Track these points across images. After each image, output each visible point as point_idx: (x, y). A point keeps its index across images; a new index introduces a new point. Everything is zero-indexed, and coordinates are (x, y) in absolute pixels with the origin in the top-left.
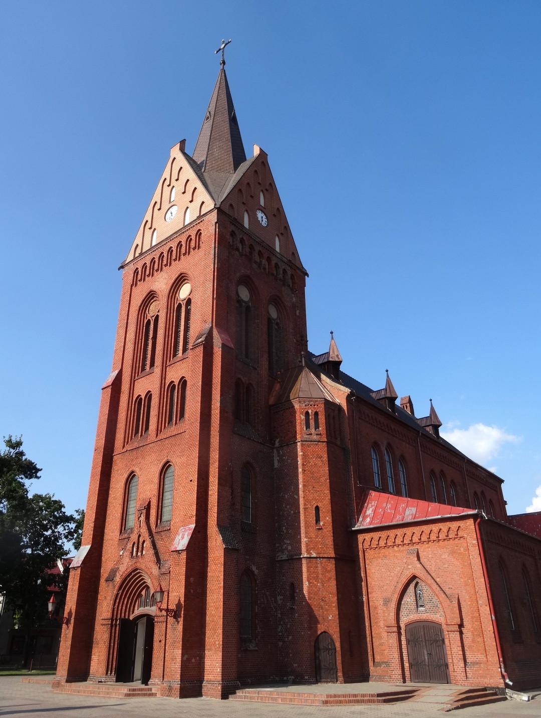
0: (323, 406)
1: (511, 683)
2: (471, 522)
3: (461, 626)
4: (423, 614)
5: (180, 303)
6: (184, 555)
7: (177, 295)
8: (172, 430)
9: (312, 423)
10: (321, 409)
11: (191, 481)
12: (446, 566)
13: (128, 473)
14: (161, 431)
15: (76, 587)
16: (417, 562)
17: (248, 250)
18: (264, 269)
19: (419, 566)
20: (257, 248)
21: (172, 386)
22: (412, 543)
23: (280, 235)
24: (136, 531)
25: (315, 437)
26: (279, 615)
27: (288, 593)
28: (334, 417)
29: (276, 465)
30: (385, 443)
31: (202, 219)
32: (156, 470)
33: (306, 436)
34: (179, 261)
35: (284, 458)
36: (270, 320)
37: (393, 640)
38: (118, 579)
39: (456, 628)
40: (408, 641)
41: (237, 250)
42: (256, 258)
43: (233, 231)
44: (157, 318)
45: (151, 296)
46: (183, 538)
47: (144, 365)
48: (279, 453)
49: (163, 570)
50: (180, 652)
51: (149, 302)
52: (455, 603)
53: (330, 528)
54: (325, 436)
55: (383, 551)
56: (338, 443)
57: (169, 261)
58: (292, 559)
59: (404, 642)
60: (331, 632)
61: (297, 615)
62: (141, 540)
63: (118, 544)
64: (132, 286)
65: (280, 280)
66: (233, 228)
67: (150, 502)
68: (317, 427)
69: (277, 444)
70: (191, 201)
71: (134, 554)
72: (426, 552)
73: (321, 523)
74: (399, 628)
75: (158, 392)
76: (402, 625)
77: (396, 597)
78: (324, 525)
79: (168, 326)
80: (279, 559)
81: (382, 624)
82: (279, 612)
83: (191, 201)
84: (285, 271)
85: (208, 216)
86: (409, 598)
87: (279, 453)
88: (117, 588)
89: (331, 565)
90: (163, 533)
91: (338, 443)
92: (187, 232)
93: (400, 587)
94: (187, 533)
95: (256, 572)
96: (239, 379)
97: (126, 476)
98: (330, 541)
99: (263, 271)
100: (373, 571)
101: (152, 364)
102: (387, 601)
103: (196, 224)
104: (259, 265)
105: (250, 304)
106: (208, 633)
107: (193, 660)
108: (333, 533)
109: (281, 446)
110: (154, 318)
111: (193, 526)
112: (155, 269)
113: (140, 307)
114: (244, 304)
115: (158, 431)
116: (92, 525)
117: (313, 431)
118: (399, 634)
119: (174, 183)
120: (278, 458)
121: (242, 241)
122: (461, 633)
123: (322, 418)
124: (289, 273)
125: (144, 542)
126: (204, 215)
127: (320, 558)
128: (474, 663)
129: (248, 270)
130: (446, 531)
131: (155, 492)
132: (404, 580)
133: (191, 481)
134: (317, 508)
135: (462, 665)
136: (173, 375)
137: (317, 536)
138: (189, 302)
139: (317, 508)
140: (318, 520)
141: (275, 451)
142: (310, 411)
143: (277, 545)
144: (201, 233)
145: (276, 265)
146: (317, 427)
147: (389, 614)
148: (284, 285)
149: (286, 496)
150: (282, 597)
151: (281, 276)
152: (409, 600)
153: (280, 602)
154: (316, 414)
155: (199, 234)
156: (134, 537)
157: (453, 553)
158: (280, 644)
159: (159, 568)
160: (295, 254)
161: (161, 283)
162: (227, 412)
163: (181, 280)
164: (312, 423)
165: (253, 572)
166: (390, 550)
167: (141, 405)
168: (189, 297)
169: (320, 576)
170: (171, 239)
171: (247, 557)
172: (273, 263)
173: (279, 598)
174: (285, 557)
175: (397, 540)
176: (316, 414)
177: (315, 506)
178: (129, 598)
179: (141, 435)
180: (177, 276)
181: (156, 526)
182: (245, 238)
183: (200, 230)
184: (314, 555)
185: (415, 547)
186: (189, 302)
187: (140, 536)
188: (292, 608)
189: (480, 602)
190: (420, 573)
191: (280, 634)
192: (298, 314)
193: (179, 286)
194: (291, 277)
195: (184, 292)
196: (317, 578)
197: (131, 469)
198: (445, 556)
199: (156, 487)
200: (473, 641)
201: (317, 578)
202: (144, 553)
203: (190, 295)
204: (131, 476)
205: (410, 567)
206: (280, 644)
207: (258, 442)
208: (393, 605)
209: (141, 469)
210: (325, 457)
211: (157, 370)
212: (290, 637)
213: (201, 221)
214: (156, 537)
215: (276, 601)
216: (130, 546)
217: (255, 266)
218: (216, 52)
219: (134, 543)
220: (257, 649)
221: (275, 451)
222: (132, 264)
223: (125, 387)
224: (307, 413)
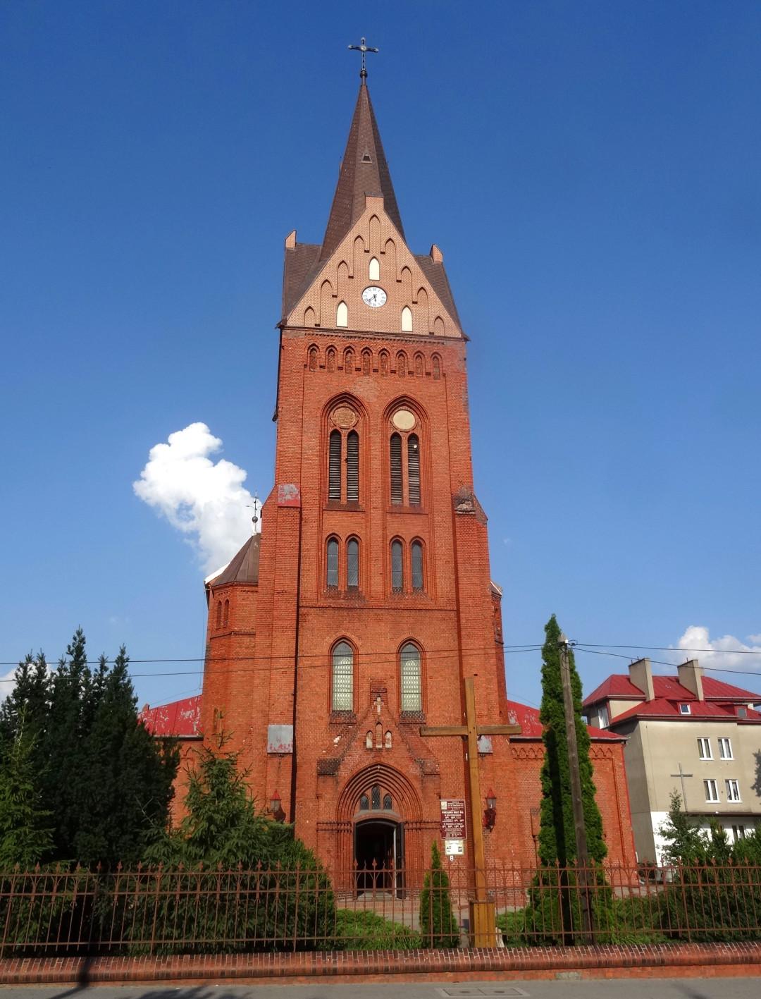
11: (476, 675)
13: (335, 637)
31: (442, 341)
64: (305, 366)
92: (415, 345)
103: (430, 342)
133: (476, 675)
138: (413, 438)
155: (435, 356)
168: (416, 432)
180: (398, 395)
193: (395, 409)
197: (340, 634)
209: (360, 638)
211: (376, 515)
218: (350, 46)
222: (304, 332)
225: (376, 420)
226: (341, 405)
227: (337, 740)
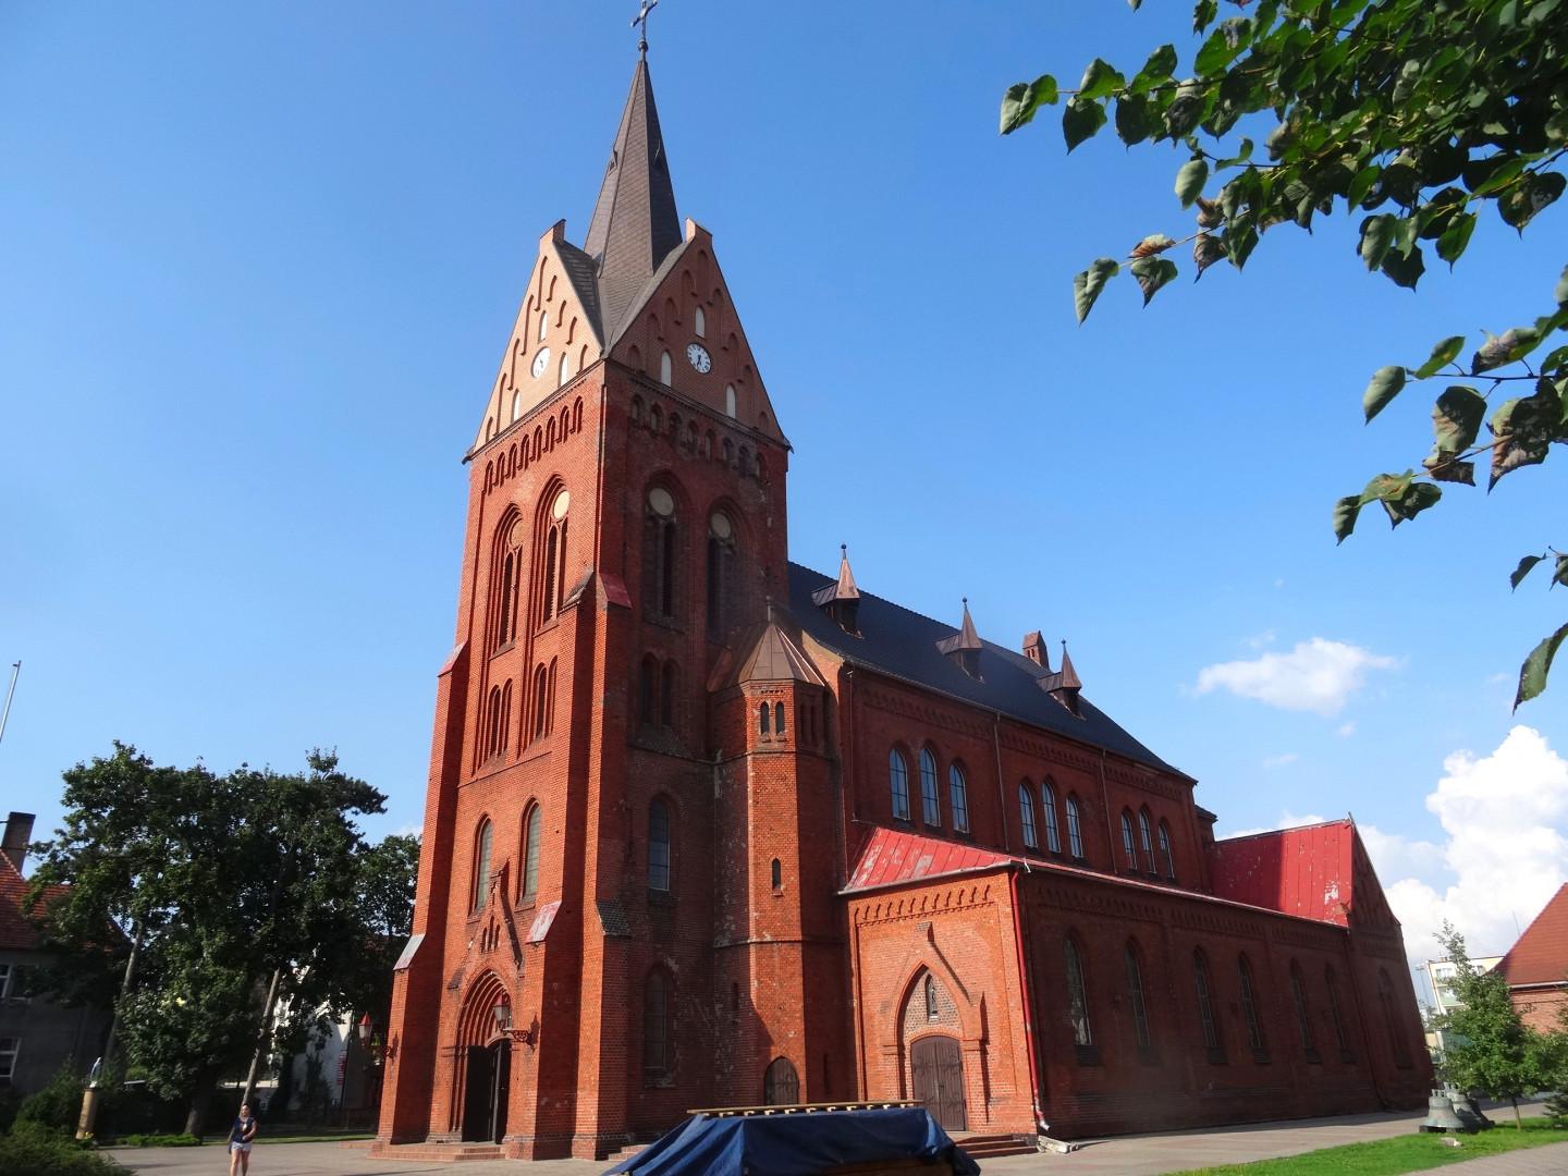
0: (791, 692)
1: (1046, 1127)
2: (1005, 876)
3: (984, 1041)
4: (936, 1026)
6: (542, 949)
7: (551, 512)
9: (772, 721)
10: (788, 697)
12: (970, 949)
14: (525, 747)
15: (403, 1001)
16: (928, 944)
17: (666, 424)
18: (702, 453)
19: (931, 949)
20: (686, 417)
23: (736, 384)
25: (776, 746)
26: (717, 1034)
27: (729, 999)
28: (813, 710)
29: (717, 793)
30: (921, 741)
32: (516, 811)
33: (762, 745)
35: (729, 781)
36: (713, 544)
37: (891, 1066)
38: (464, 986)
39: (977, 1045)
40: (914, 1069)
42: (685, 434)
43: (637, 396)
45: (511, 514)
46: (543, 922)
48: (721, 772)
50: (535, 1093)
51: (511, 522)
52: (977, 1005)
53: (796, 894)
54: (792, 742)
55: (884, 926)
56: (820, 751)
58: (736, 946)
59: (908, 1070)
60: (792, 1056)
61: (741, 1032)
63: (466, 931)
64: (483, 494)
66: (637, 389)
67: (508, 864)
68: (780, 728)
69: (719, 759)
70: (569, 343)
71: (486, 947)
73: (782, 887)
74: (901, 1047)
76: (907, 1043)
77: (897, 1000)
78: (786, 889)
79: (535, 567)
82: (717, 1028)
83: (569, 343)
86: (917, 1002)
87: (721, 772)
88: (462, 999)
89: (796, 954)
90: (525, 914)
91: (820, 751)
93: (904, 983)
94: (548, 916)
95: (675, 968)
97: (476, 821)
98: (795, 914)
99: (698, 457)
100: (869, 959)
102: (886, 1006)
105: (675, 519)
106: (582, 1065)
107: (558, 1105)
108: (801, 901)
111: (558, 903)
112: (530, 456)
113: (496, 531)
114: (661, 522)
115: (521, 748)
116: (427, 901)
117: (773, 735)
118: (901, 1056)
119: (545, 305)
120: (720, 782)
121: (656, 409)
122: (984, 1052)
123: (789, 714)
126: (588, 368)
127: (777, 942)
128: (1000, 1099)
131: (516, 848)
132: (909, 972)
134: (776, 863)
135: (982, 1102)
137: (774, 908)
139: (776, 863)
140: (776, 882)
141: (716, 768)
142: (769, 702)
143: (716, 924)
145: (727, 442)
146: (780, 728)
147: (887, 1027)
150: (721, 1006)
152: (916, 1003)
153: (718, 1013)
154: (780, 705)
155: (579, 403)
156: (486, 921)
157: (979, 928)
158: (718, 1077)
159: (519, 968)
161: (524, 490)
162: (617, 717)
163: (553, 487)
164: (772, 721)
165: (669, 969)
166: (894, 925)
167: (497, 700)
169: (777, 971)
171: (659, 946)
172: (720, 438)
173: (718, 1006)
174: (726, 943)
175: (902, 910)
176: (780, 705)
177: (772, 859)
178: (482, 1015)
179: (499, 754)
180: (547, 479)
181: (517, 902)
182: (661, 404)
184: (768, 938)
187: (493, 918)
188: (734, 1022)
189: (1011, 1004)
191: (718, 1062)
196: (771, 975)
197: (482, 811)
198: (969, 933)
199: (516, 840)
200: (1001, 1063)
201: (771, 975)
204: (484, 823)
205: (918, 952)
206: (718, 1077)
208: (893, 1012)
210: (792, 776)
211: (520, 644)
212: (732, 1067)
214: (517, 919)
215: (712, 1012)
216: (480, 933)
217: (682, 451)
219: (485, 930)
220: (673, 1086)
224: (765, 704)
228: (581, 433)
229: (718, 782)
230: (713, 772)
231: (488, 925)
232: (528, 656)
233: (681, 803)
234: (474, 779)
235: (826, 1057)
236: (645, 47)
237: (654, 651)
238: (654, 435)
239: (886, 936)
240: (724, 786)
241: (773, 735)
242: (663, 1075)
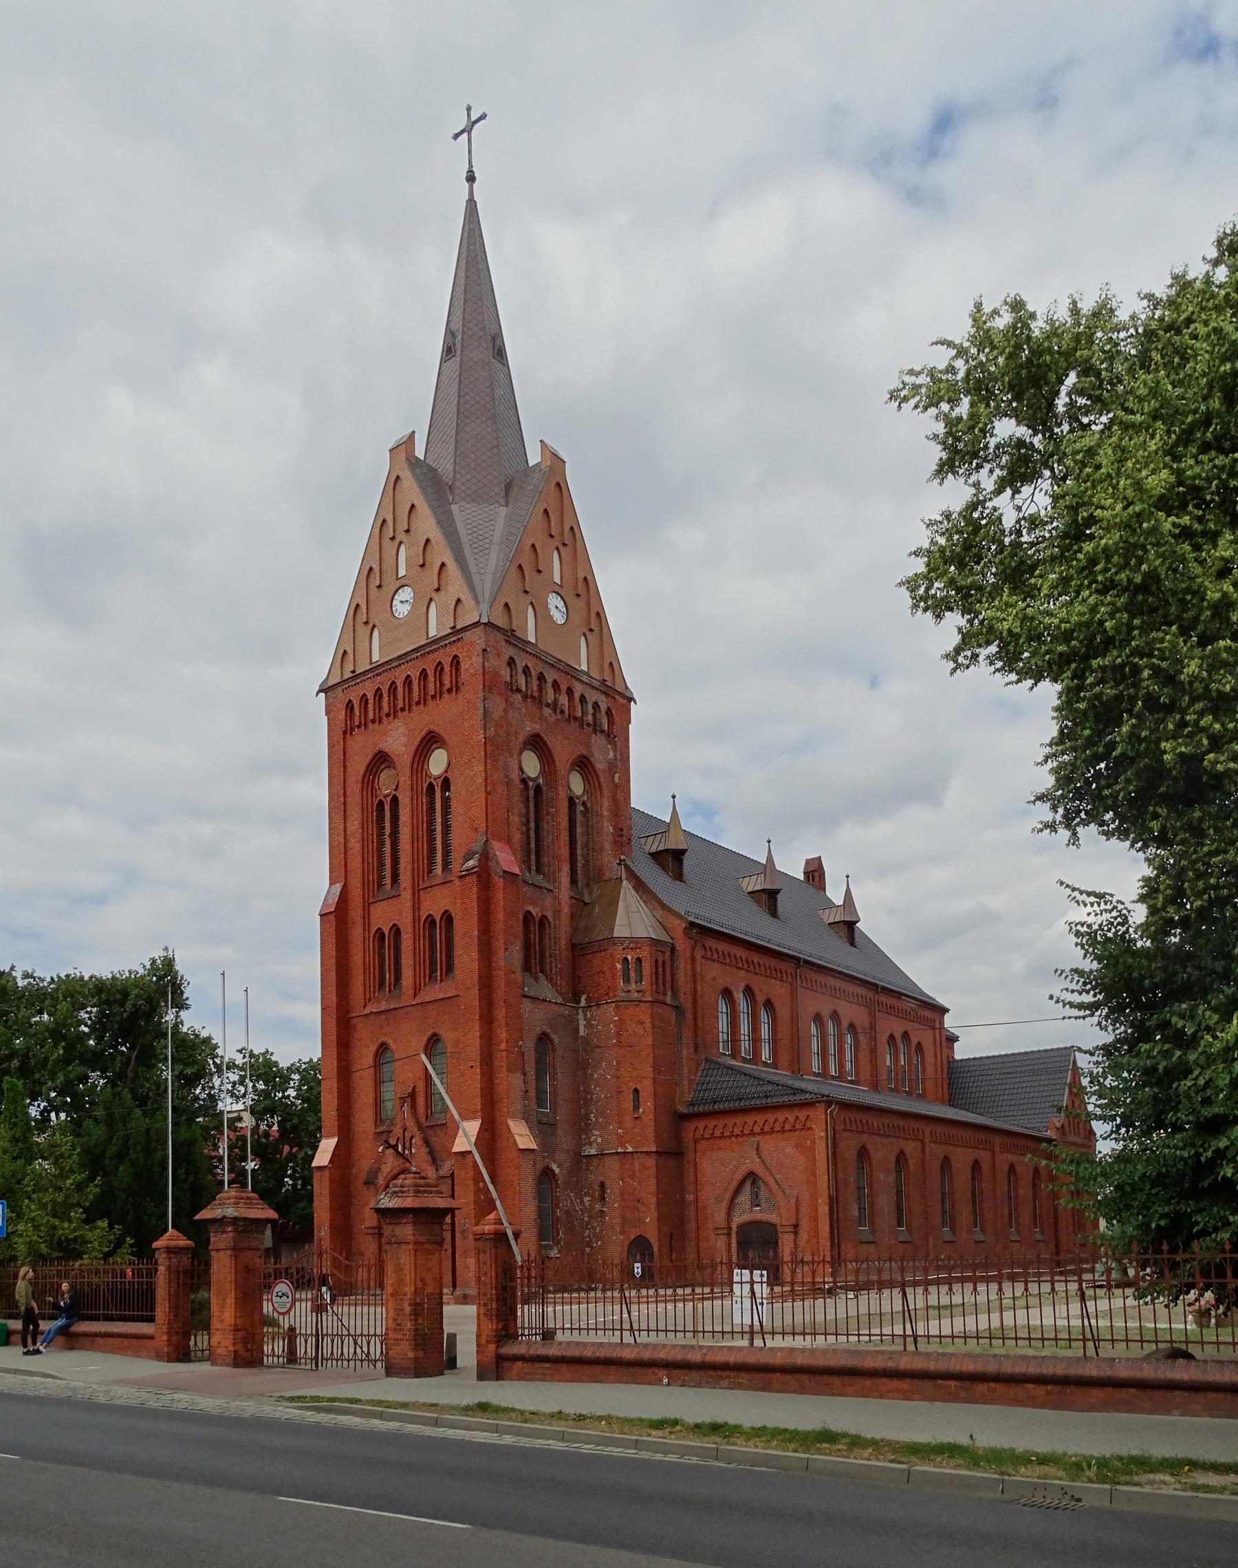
3: (796, 1226)
4: (758, 1214)
5: (431, 783)
7: (425, 766)
8: (435, 991)
9: (632, 974)
13: (377, 1044)
14: (420, 989)
17: (535, 683)
18: (562, 712)
20: (550, 676)
21: (431, 921)
22: (752, 1133)
24: (399, 1125)
26: (586, 1219)
27: (597, 1194)
28: (664, 963)
29: (582, 1032)
34: (425, 704)
36: (571, 801)
37: (721, 1242)
40: (739, 1243)
41: (519, 690)
42: (550, 697)
44: (395, 800)
45: (381, 760)
47: (381, 878)
48: (585, 1015)
49: (442, 1173)
51: (378, 768)
52: (793, 1201)
53: (651, 1116)
54: (649, 993)
55: (719, 1141)
56: (668, 1000)
57: (407, 701)
60: (648, 1236)
62: (408, 1135)
63: (375, 1139)
64: (345, 733)
65: (588, 725)
66: (509, 651)
69: (583, 1003)
70: (438, 590)
72: (769, 1145)
73: (641, 1110)
74: (730, 1228)
75: (411, 930)
76: (734, 1227)
77: (729, 1195)
79: (415, 821)
80: (586, 1153)
81: (710, 1225)
83: (438, 590)
84: (596, 706)
85: (468, 634)
86: (744, 1198)
91: (668, 1000)
93: (735, 1184)
95: (557, 1170)
96: (529, 912)
97: (373, 1048)
98: (650, 1132)
99: (559, 716)
101: (395, 878)
102: (719, 1199)
104: (554, 706)
105: (541, 781)
109: (589, 1006)
110: (389, 799)
114: (531, 784)
115: (417, 990)
116: (334, 1113)
117: (633, 986)
118: (729, 1235)
119: (401, 536)
122: (796, 1233)
123: (647, 968)
124: (603, 707)
125: (412, 1138)
126: (462, 629)
127: (637, 1152)
129: (536, 723)
130: (792, 1121)
132: (739, 1176)
136: (434, 905)
141: (580, 1011)
142: (629, 958)
143: (584, 1137)
144: (458, 662)
145: (583, 699)
148: (595, 731)
149: (596, 1075)
151: (590, 718)
152: (743, 1199)
153: (587, 1204)
154: (639, 960)
157: (797, 1146)
158: (588, 1250)
159: (437, 1170)
160: (614, 667)
162: (514, 972)
163: (430, 741)
165: (552, 1171)
166: (727, 1141)
169: (637, 1174)
170: (408, 659)
172: (577, 695)
173: (586, 1199)
174: (593, 1152)
179: (390, 991)
181: (427, 1118)
182: (529, 665)
183: (456, 656)
184: (630, 1149)
185: (755, 1139)
186: (446, 785)
187: (405, 1129)
188: (602, 1211)
190: (760, 1171)
192: (617, 780)
194: (607, 713)
195: (437, 763)
196: (633, 1176)
197: (380, 1041)
198: (790, 1150)
201: (633, 1176)
202: (413, 1151)
203: (446, 771)
204: (383, 1048)
207: (556, 1003)
208: (725, 1204)
209: (395, 1041)
211: (407, 895)
213: (459, 640)
215: (582, 1203)
217: (547, 712)
219: (398, 1139)
221: (580, 1011)
222: (340, 689)
223: (356, 912)
224: (626, 959)
225: (405, 780)
226: (382, 767)
227: (380, 1150)
228: (460, 695)
229: (582, 1023)
230: (577, 1014)
231: (400, 1135)
232: (416, 906)
233: (556, 1041)
234: (367, 1011)
235: (671, 1235)
236: (471, 178)
237: (531, 908)
238: (525, 697)
239: (720, 1149)
240: (588, 1026)
241: (633, 986)
242: (551, 1248)
